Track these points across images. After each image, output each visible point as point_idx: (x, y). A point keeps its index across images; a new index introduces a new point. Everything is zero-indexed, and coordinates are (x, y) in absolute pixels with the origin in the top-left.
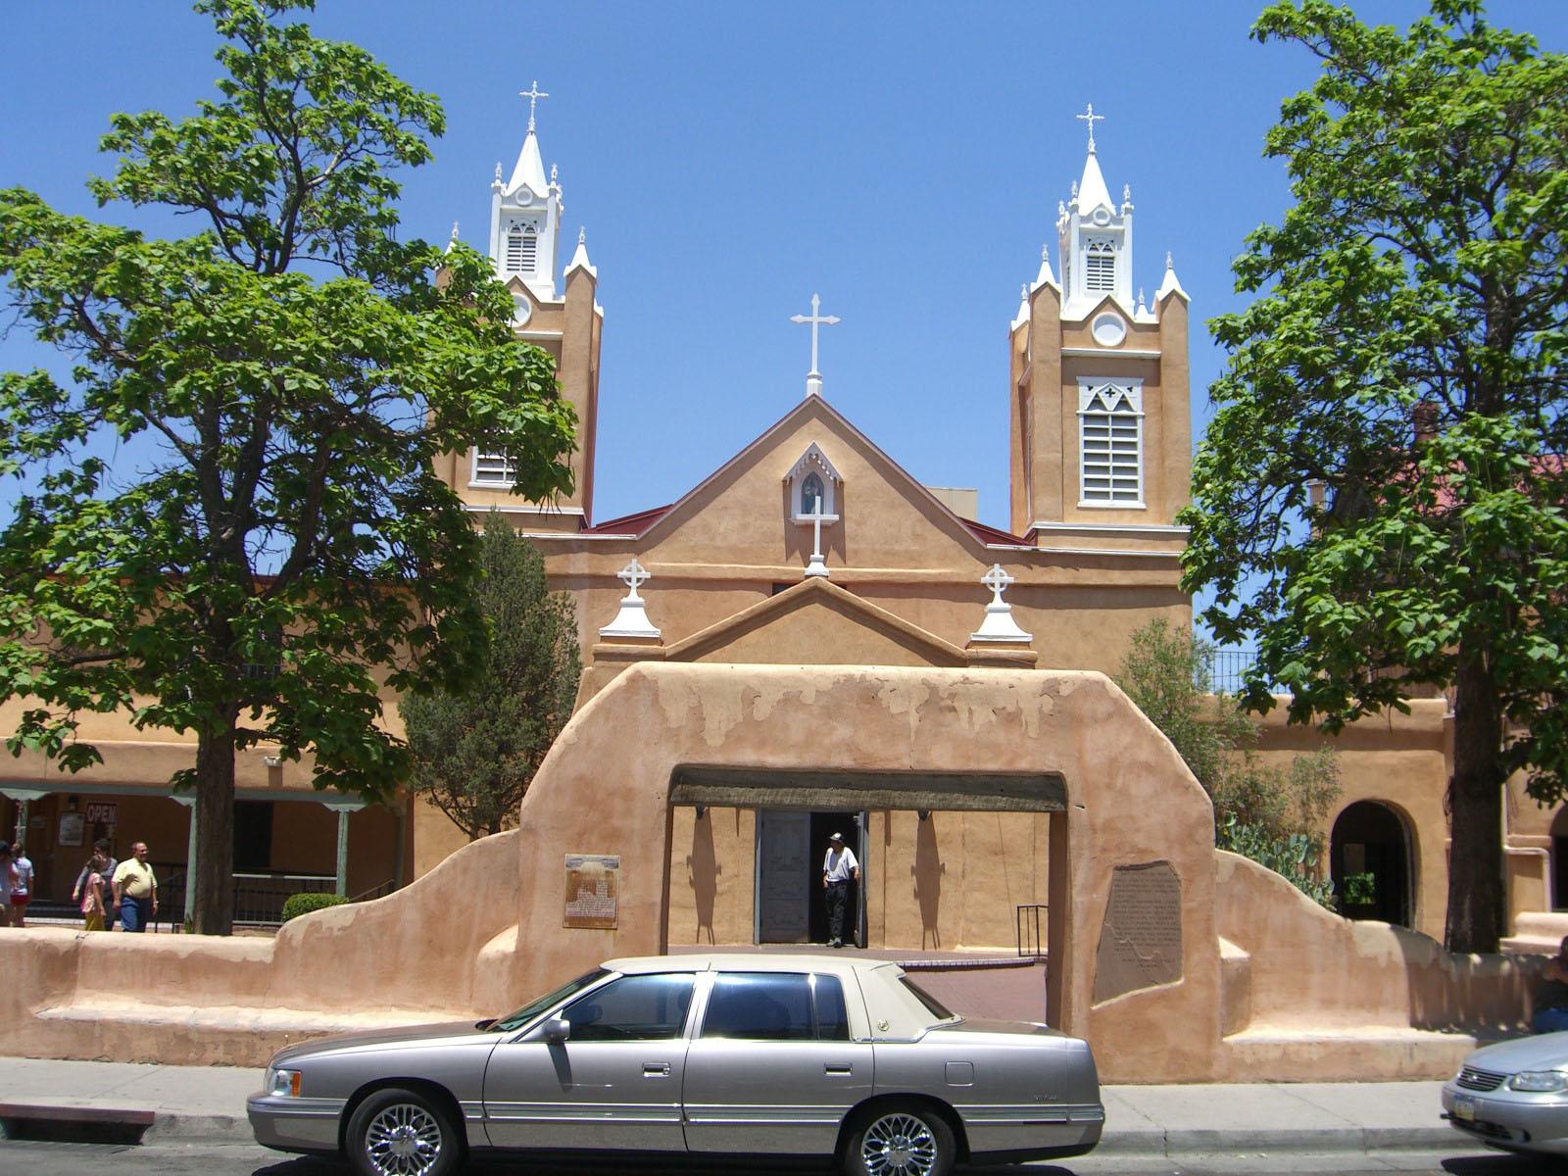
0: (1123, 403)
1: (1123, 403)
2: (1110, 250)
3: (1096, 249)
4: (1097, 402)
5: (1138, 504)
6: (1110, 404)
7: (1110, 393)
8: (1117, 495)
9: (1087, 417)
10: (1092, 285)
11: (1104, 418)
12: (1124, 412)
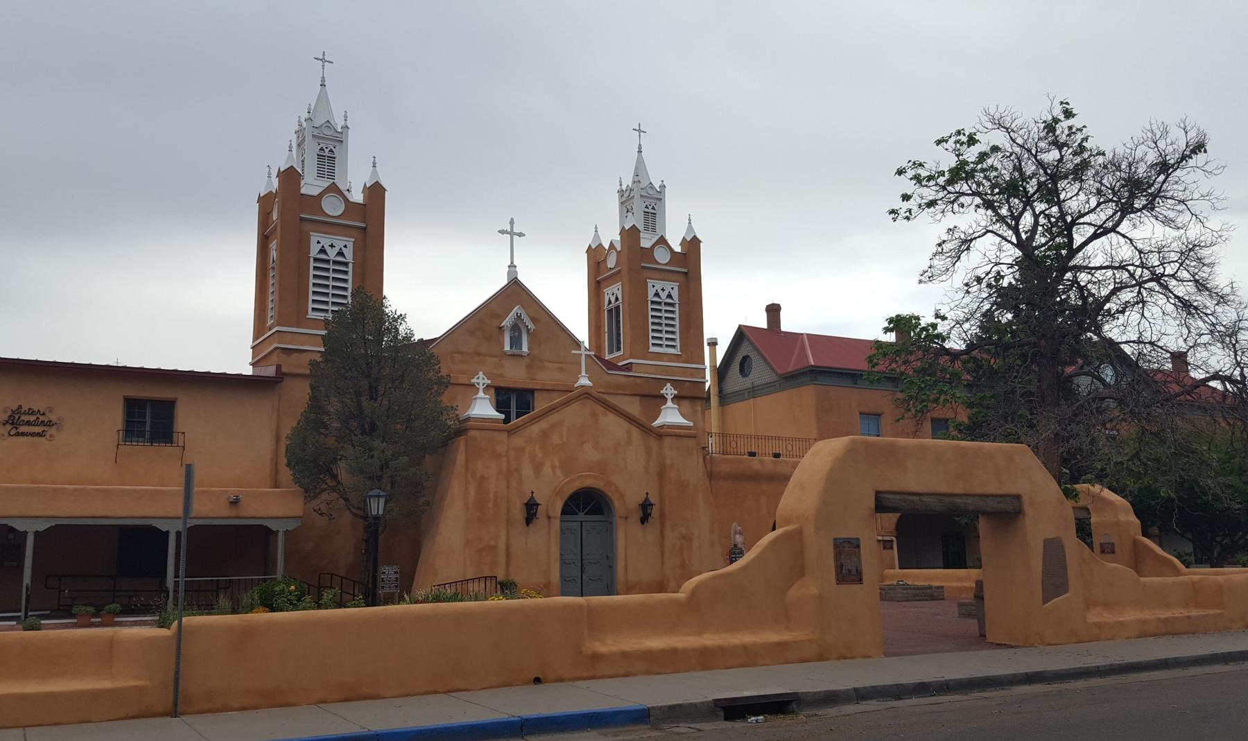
0: (340, 253)
6: (332, 254)
7: (332, 246)
9: (316, 260)
10: (320, 175)
11: (327, 261)
12: (340, 259)
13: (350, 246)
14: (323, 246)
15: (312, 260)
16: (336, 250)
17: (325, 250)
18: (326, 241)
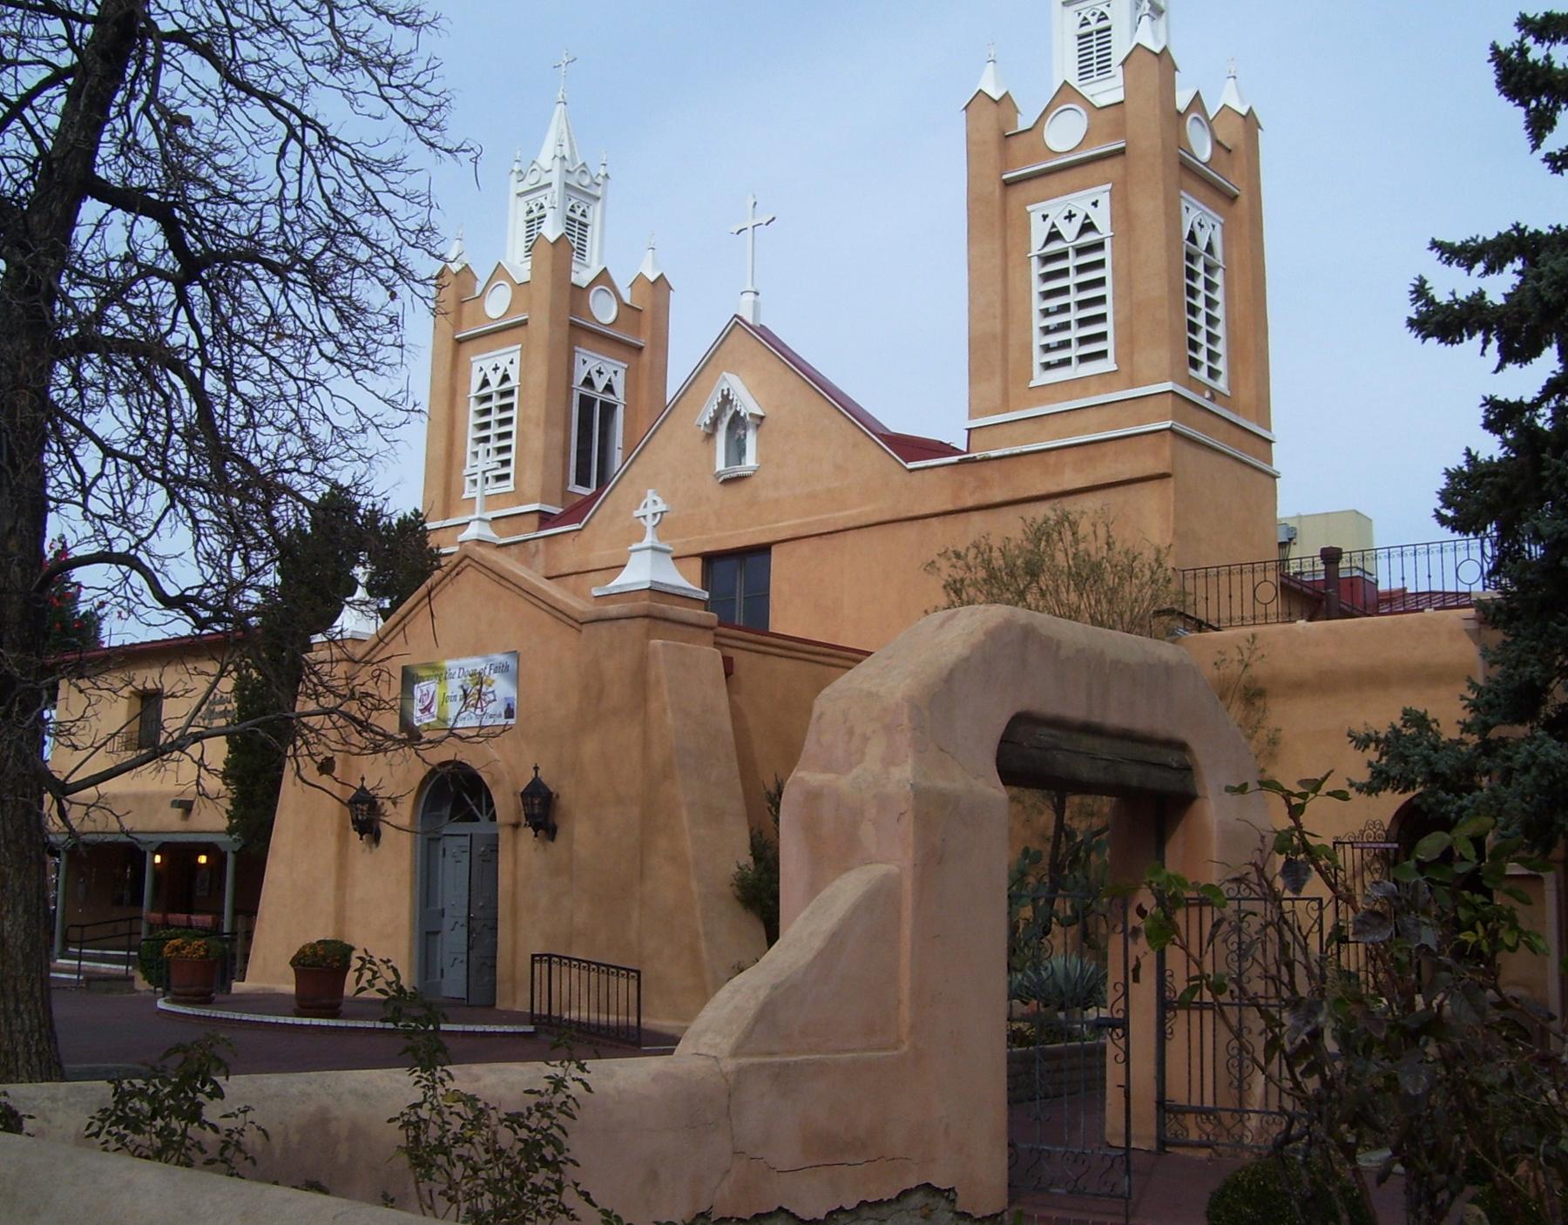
0: (1088, 227)
1: (1088, 227)
2: (1106, 18)
3: (1089, 23)
4: (1054, 236)
5: (1107, 365)
6: (1069, 231)
8: (1083, 359)
11: (1063, 255)
13: (1105, 201)
14: (1054, 226)
15: (1035, 261)
16: (1077, 223)
17: (1058, 232)
18: (1056, 209)
